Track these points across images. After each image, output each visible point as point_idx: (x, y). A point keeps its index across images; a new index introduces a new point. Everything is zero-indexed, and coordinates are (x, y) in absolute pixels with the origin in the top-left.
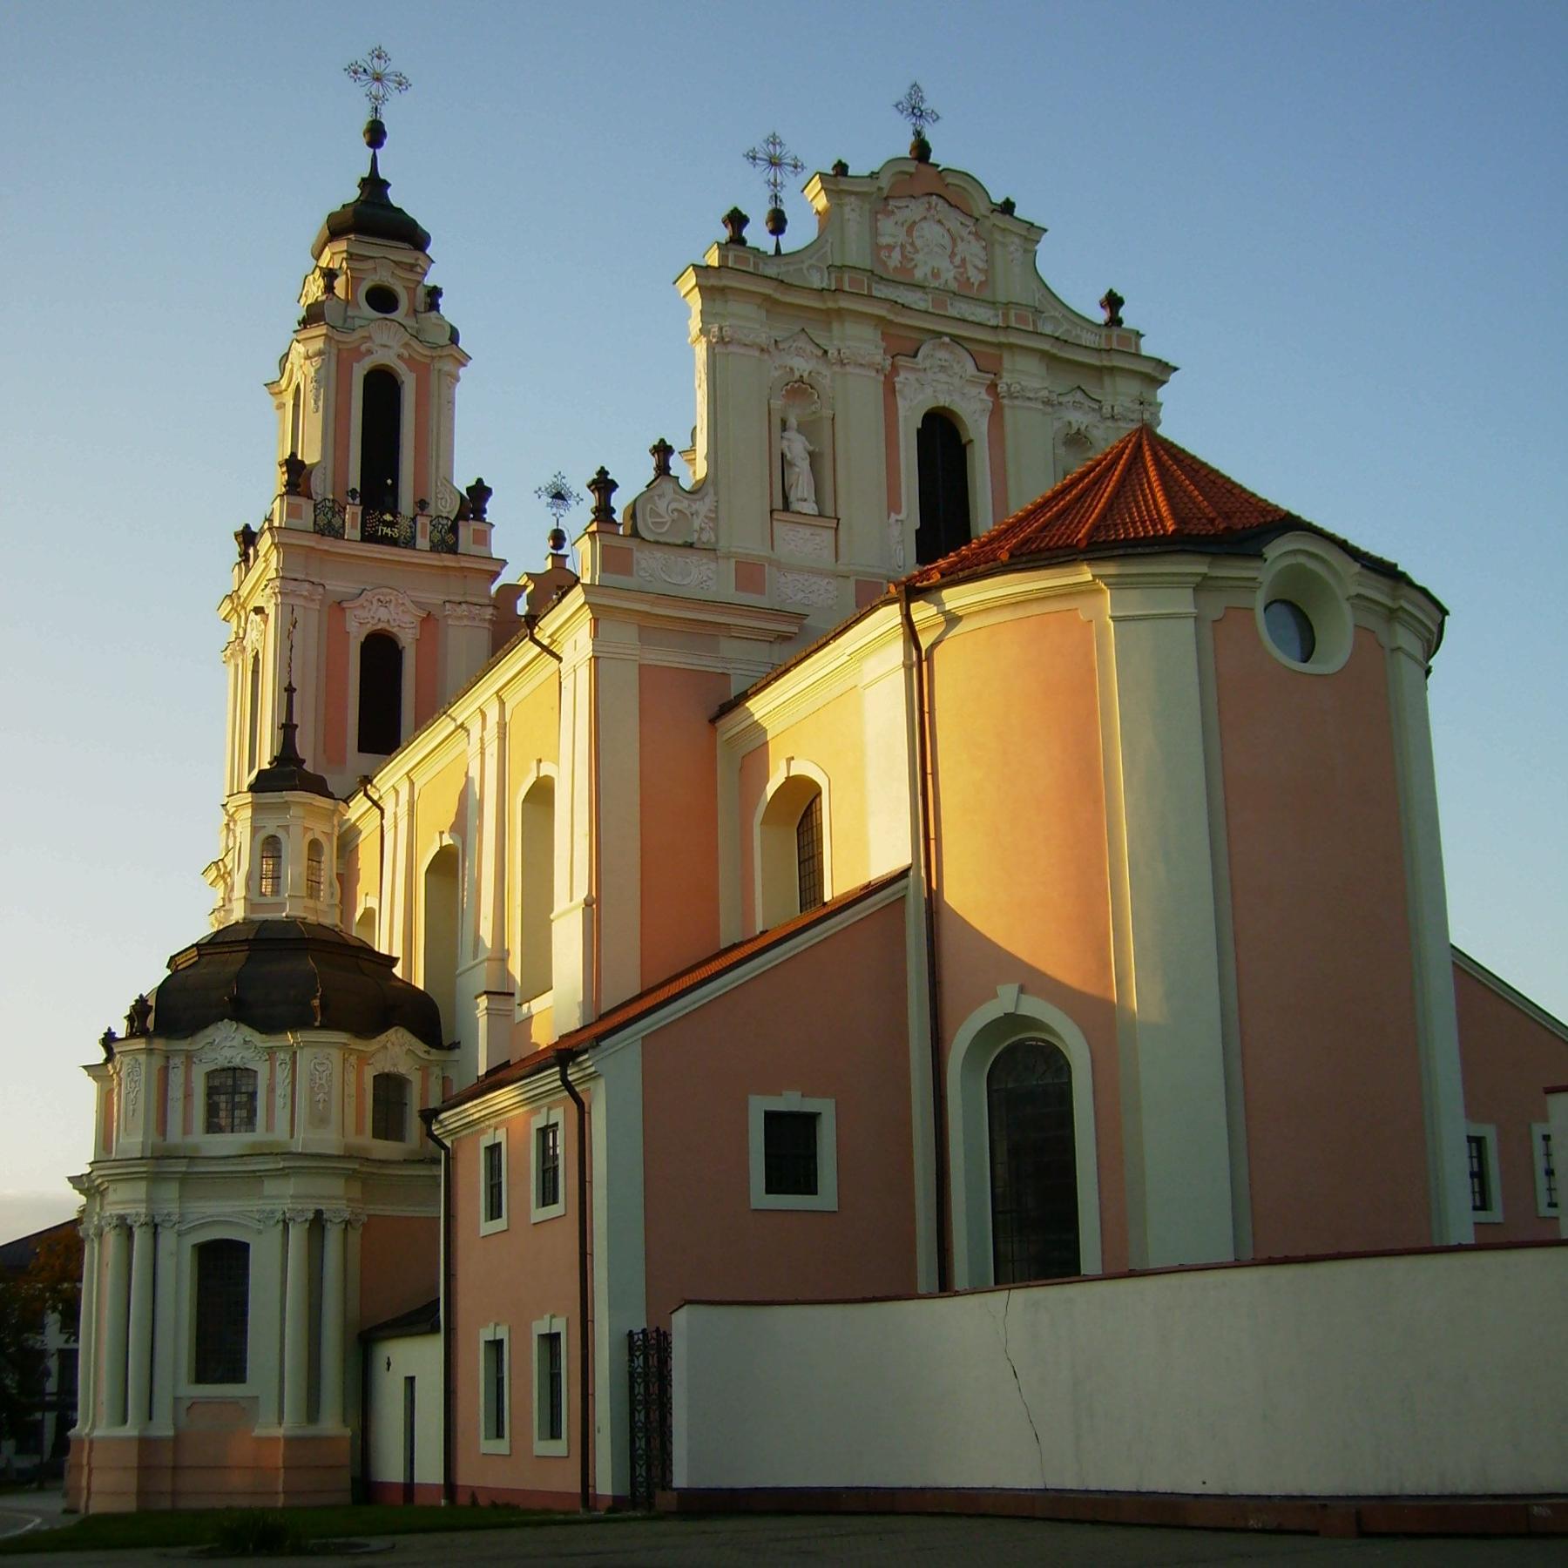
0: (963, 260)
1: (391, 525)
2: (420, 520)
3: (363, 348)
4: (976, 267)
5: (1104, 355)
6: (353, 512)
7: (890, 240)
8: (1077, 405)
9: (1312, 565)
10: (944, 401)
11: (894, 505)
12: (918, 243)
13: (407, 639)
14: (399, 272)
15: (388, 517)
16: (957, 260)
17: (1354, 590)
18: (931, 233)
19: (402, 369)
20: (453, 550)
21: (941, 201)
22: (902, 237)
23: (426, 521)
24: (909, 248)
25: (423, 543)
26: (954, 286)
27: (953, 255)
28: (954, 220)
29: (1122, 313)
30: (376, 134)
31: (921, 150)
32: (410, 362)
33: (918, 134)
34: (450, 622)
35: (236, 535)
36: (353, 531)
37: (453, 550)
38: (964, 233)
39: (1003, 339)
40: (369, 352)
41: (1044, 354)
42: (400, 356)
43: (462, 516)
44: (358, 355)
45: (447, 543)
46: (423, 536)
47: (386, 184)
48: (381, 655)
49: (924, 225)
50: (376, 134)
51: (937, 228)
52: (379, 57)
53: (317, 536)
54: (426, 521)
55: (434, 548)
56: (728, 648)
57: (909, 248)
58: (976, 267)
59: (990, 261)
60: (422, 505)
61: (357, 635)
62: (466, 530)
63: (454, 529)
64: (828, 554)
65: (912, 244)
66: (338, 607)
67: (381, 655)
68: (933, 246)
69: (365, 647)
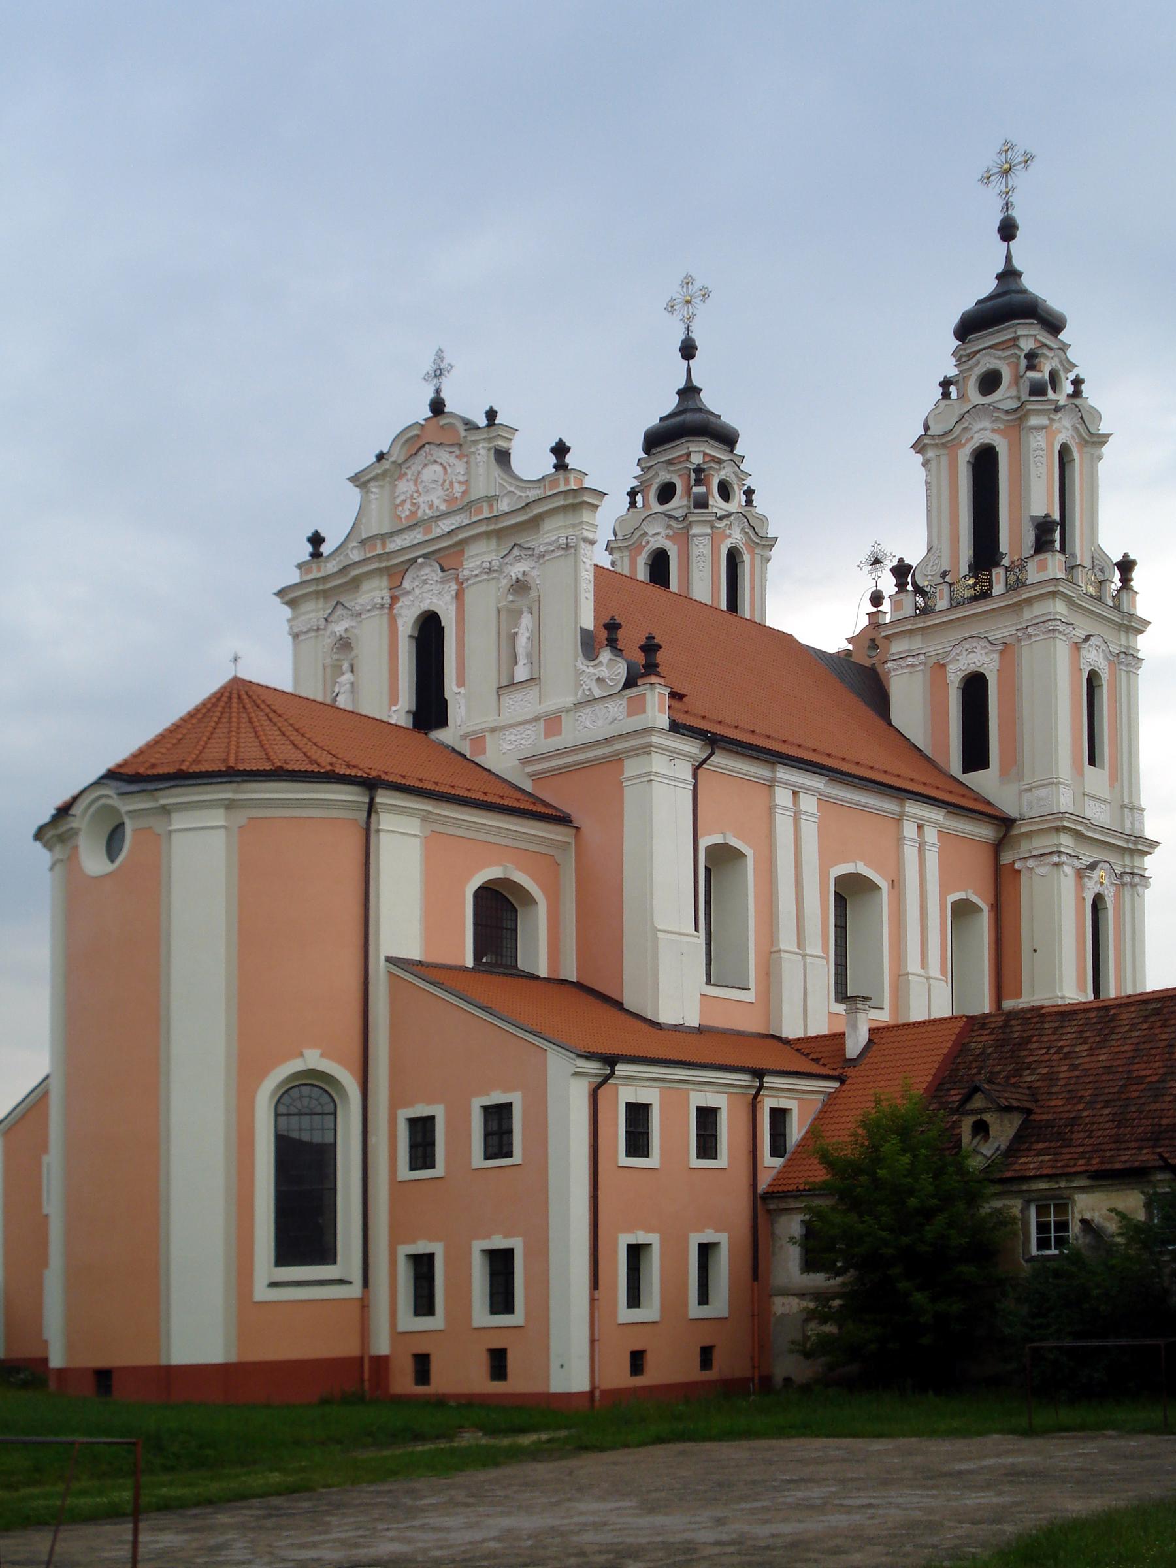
0: (451, 483)
4: (459, 482)
5: (528, 510)
7: (402, 498)
8: (518, 559)
10: (425, 606)
16: (447, 485)
18: (432, 472)
21: (432, 446)
26: (443, 507)
28: (443, 456)
31: (437, 407)
33: (438, 391)
38: (452, 460)
39: (456, 539)
41: (488, 534)
47: (699, 390)
49: (425, 471)
50: (688, 350)
58: (459, 482)
59: (468, 472)
68: (433, 483)
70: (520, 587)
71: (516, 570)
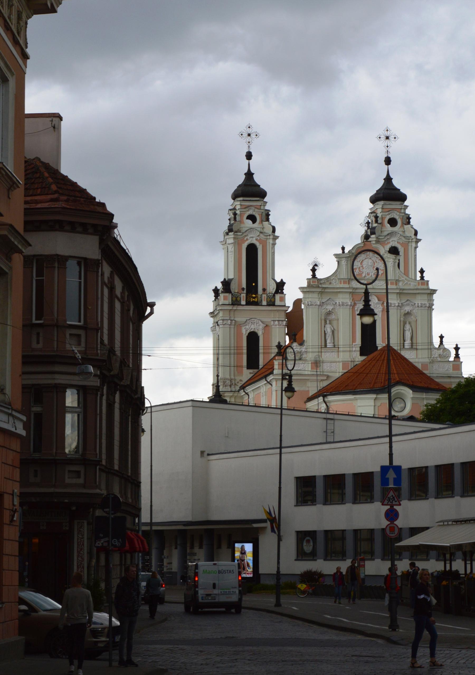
1: (254, 298)
2: (263, 295)
3: (245, 239)
6: (243, 296)
9: (402, 391)
11: (354, 340)
12: (364, 266)
13: (260, 333)
14: (256, 210)
15: (254, 296)
17: (412, 396)
19: (257, 244)
20: (273, 305)
22: (360, 265)
23: (265, 295)
24: (361, 268)
25: (264, 303)
27: (374, 267)
29: (424, 275)
30: (249, 156)
32: (260, 241)
34: (273, 326)
35: (214, 290)
36: (243, 302)
37: (273, 305)
40: (247, 240)
42: (256, 240)
43: (277, 292)
44: (244, 241)
45: (271, 303)
46: (264, 301)
48: (253, 338)
50: (249, 156)
51: (370, 261)
52: (249, 127)
53: (232, 306)
54: (265, 295)
55: (268, 305)
56: (309, 384)
57: (361, 268)
60: (264, 290)
61: (245, 332)
62: (278, 297)
63: (274, 296)
64: (336, 356)
65: (362, 267)
66: (238, 326)
67: (253, 338)
69: (248, 337)
70: (408, 314)
71: (407, 309)
